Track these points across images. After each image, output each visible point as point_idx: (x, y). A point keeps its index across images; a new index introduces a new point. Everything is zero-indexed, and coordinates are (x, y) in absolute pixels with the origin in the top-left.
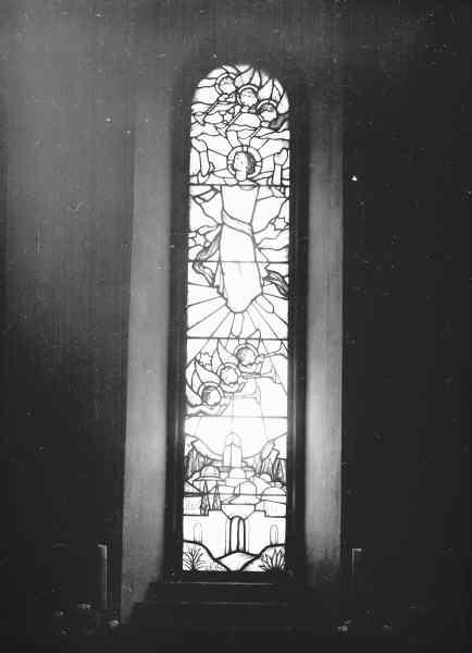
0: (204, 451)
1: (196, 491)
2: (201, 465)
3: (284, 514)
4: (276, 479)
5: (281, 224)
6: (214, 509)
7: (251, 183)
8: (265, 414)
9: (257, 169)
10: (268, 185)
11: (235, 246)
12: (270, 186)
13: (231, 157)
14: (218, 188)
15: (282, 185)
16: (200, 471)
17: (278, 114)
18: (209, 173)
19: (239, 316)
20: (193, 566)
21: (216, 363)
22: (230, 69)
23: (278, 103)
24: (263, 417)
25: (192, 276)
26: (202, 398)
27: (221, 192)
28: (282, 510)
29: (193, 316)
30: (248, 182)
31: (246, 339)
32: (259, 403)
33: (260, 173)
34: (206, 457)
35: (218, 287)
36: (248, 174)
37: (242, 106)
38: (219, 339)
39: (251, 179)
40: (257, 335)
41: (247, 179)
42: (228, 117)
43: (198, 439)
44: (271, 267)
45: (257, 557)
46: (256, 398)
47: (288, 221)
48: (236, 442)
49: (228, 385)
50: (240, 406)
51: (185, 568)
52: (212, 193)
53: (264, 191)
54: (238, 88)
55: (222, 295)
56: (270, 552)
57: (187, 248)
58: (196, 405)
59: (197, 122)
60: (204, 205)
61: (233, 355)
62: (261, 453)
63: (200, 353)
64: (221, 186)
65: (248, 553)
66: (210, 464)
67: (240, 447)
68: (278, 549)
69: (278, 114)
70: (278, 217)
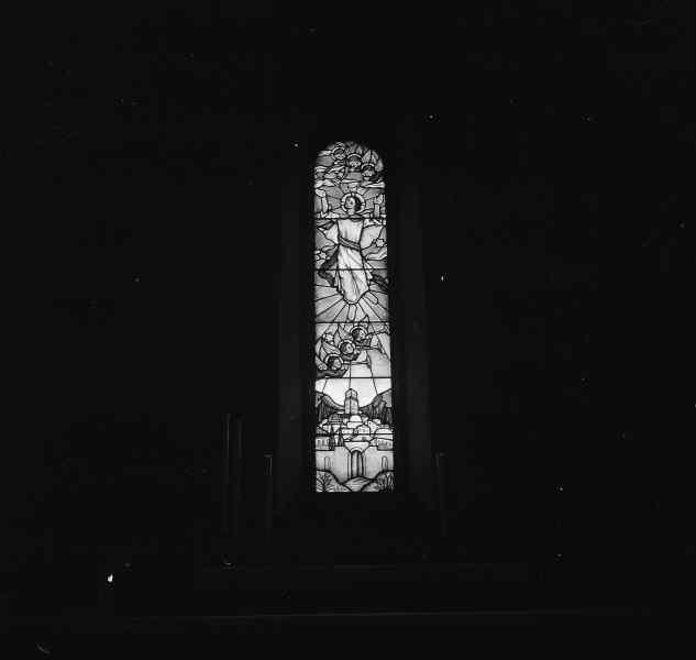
4: (384, 422)
5: (380, 243)
11: (348, 259)
12: (371, 219)
18: (328, 211)
21: (337, 339)
25: (320, 281)
34: (332, 408)
40: (366, 320)
42: (341, 175)
44: (376, 273)
48: (355, 396)
50: (358, 370)
51: (319, 491)
62: (373, 403)
67: (357, 400)
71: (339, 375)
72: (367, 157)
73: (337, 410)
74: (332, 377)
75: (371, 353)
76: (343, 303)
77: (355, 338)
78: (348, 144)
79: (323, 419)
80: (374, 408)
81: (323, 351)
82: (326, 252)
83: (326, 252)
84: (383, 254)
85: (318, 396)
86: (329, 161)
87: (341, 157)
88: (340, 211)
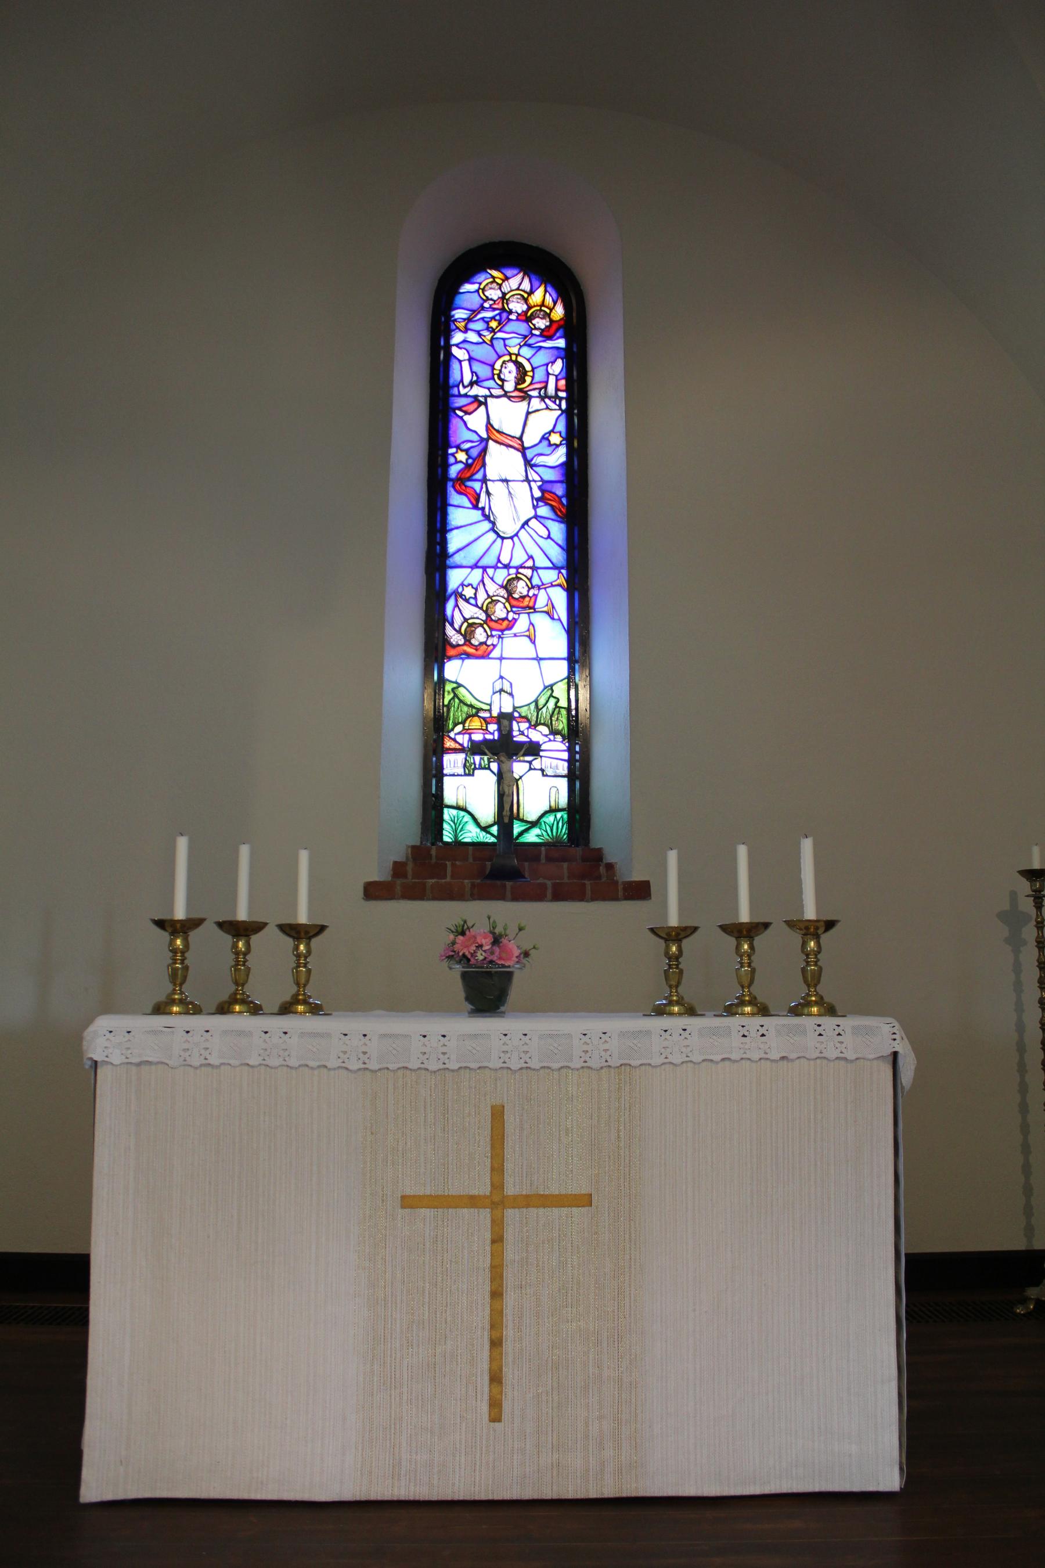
0: (469, 699)
1: (458, 746)
2: (464, 716)
3: (565, 772)
4: (554, 732)
5: (555, 439)
6: (481, 768)
7: (522, 394)
8: (540, 656)
9: (528, 380)
10: (540, 396)
12: (542, 398)
13: (497, 366)
14: (482, 399)
15: (557, 396)
16: (463, 723)
17: (551, 321)
18: (472, 384)
19: (508, 543)
20: (456, 836)
21: (482, 596)
22: (495, 273)
23: (551, 310)
24: (538, 659)
25: (455, 498)
26: (464, 636)
27: (486, 404)
28: (563, 768)
29: (455, 541)
30: (516, 394)
31: (517, 568)
32: (534, 642)
33: (531, 384)
34: (471, 706)
35: (483, 509)
36: (517, 384)
37: (511, 312)
38: (484, 569)
39: (521, 390)
40: (530, 563)
41: (516, 389)
42: (494, 324)
43: (460, 685)
44: (548, 487)
45: (534, 824)
46: (529, 637)
47: (564, 434)
48: (507, 688)
49: (496, 621)
50: (513, 645)
51: (446, 839)
52: (475, 405)
53: (536, 403)
54: (504, 294)
55: (487, 517)
56: (550, 819)
57: (446, 466)
58: (459, 645)
59: (457, 328)
60: (466, 418)
61: (502, 586)
62: (536, 701)
63: (462, 585)
64: (486, 397)
65: (522, 820)
66: (476, 715)
67: (511, 694)
68: (559, 815)
69: (551, 321)
70: (553, 431)
71: (483, 653)
72: (537, 297)
73: (479, 710)
74: (469, 656)
75: (535, 617)
76: (492, 536)
77: (510, 594)
78: (509, 272)
79: (455, 725)
80: (538, 709)
81: (457, 612)
82: (467, 451)
83: (467, 451)
84: (560, 456)
85: (449, 687)
86: (475, 301)
87: (494, 294)
88: (490, 384)
